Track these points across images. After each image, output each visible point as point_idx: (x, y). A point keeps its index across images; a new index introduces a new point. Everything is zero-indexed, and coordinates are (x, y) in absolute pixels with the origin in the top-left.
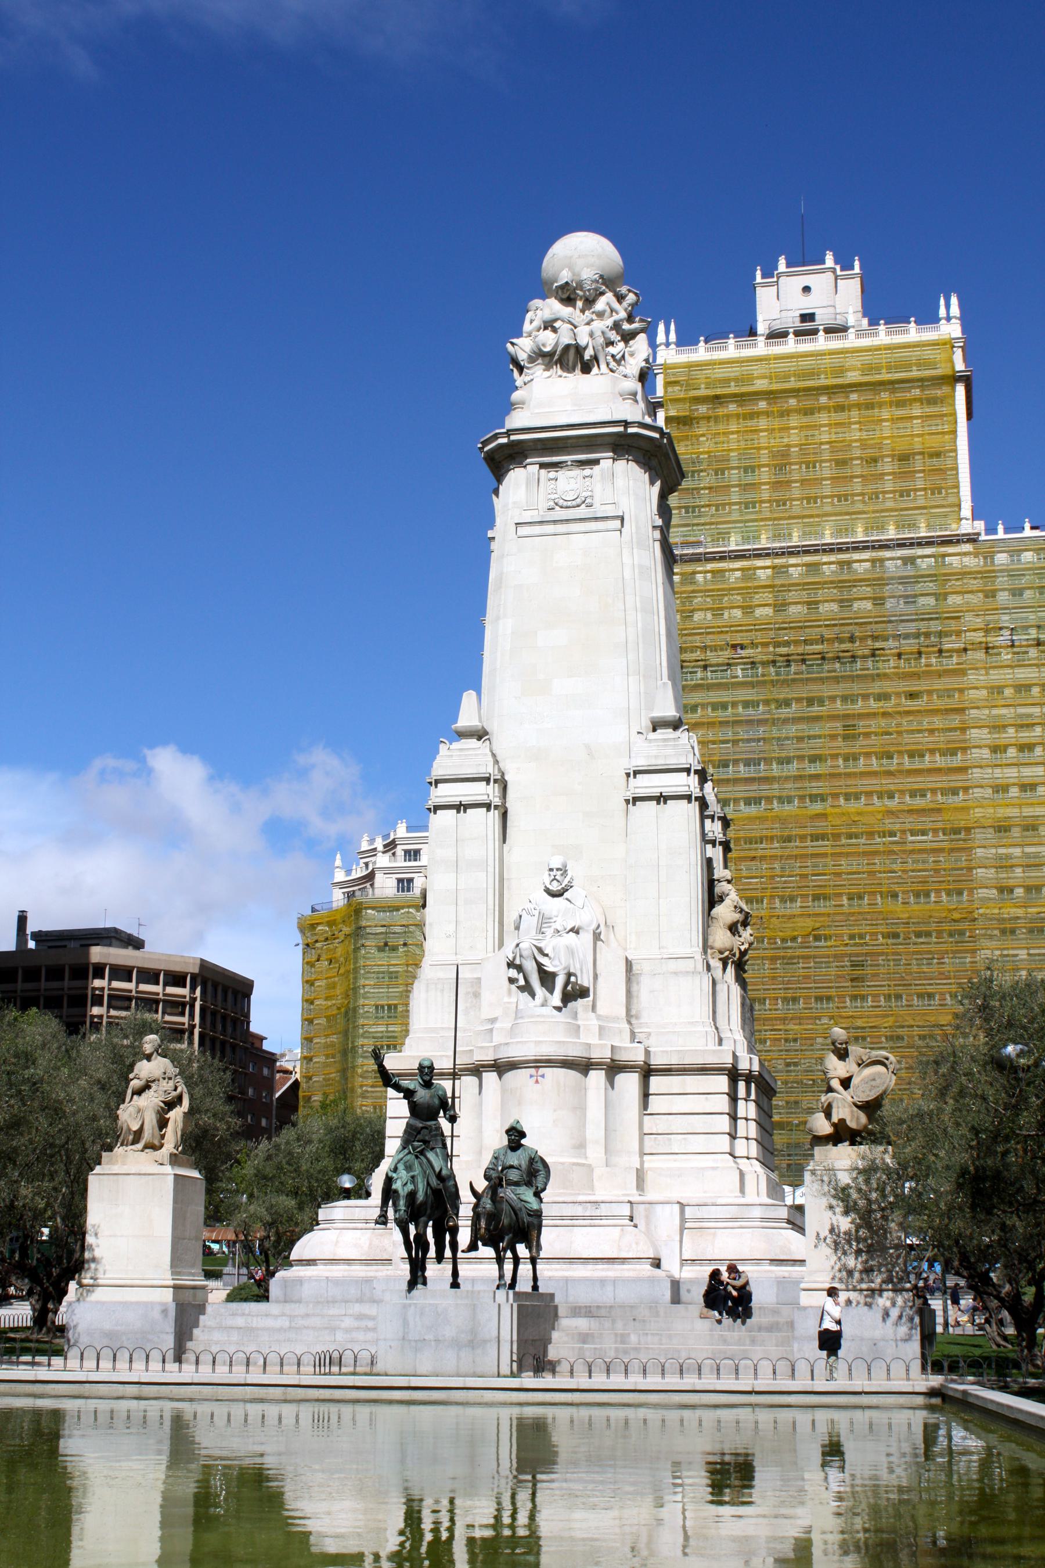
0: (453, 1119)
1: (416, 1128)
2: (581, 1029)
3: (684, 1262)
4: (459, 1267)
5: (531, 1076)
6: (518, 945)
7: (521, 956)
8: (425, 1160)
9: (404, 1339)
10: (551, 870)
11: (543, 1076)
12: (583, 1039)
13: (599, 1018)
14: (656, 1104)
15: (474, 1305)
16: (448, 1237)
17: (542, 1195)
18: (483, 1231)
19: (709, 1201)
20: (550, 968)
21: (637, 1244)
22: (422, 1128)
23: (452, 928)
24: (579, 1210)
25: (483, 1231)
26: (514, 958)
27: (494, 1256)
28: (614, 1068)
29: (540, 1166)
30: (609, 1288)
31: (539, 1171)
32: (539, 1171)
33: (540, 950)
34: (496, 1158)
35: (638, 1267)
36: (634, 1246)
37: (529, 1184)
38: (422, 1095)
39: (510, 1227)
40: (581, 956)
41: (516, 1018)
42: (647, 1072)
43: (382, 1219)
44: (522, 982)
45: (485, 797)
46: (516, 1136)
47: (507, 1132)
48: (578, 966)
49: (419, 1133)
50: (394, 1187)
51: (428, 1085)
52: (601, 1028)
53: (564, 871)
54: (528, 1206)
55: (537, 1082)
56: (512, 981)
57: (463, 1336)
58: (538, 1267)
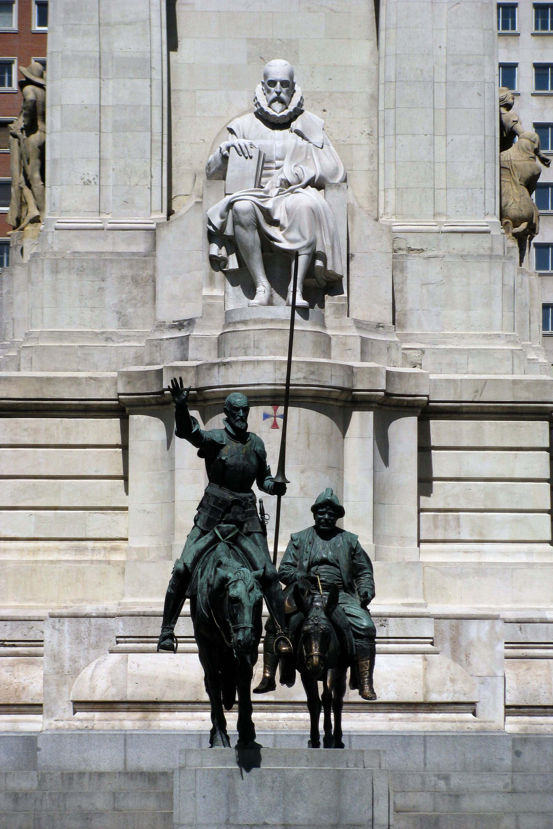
0: (279, 489)
1: (225, 501)
2: (333, 342)
3: (512, 710)
4: (255, 716)
5: (266, 416)
6: (230, 205)
7: (235, 223)
8: (239, 551)
9: (227, 822)
10: (273, 83)
12: (337, 358)
13: (359, 324)
14: (441, 463)
15: (340, 775)
17: (369, 607)
18: (316, 659)
19: (535, 615)
21: (453, 681)
23: (92, 170)
25: (316, 659)
26: (223, 225)
27: (304, 697)
28: (389, 407)
30: (417, 749)
31: (362, 568)
32: (363, 568)
33: (267, 213)
34: (296, 548)
35: (454, 716)
36: (449, 684)
37: (350, 589)
38: (230, 453)
39: (334, 656)
40: (332, 226)
41: (228, 324)
42: (427, 412)
43: (168, 642)
46: (328, 513)
47: (315, 509)
48: (327, 242)
49: (228, 510)
50: (233, 592)
51: (240, 434)
52: (364, 341)
53: (288, 85)
56: (216, 263)
57: (323, 817)
58: (344, 715)
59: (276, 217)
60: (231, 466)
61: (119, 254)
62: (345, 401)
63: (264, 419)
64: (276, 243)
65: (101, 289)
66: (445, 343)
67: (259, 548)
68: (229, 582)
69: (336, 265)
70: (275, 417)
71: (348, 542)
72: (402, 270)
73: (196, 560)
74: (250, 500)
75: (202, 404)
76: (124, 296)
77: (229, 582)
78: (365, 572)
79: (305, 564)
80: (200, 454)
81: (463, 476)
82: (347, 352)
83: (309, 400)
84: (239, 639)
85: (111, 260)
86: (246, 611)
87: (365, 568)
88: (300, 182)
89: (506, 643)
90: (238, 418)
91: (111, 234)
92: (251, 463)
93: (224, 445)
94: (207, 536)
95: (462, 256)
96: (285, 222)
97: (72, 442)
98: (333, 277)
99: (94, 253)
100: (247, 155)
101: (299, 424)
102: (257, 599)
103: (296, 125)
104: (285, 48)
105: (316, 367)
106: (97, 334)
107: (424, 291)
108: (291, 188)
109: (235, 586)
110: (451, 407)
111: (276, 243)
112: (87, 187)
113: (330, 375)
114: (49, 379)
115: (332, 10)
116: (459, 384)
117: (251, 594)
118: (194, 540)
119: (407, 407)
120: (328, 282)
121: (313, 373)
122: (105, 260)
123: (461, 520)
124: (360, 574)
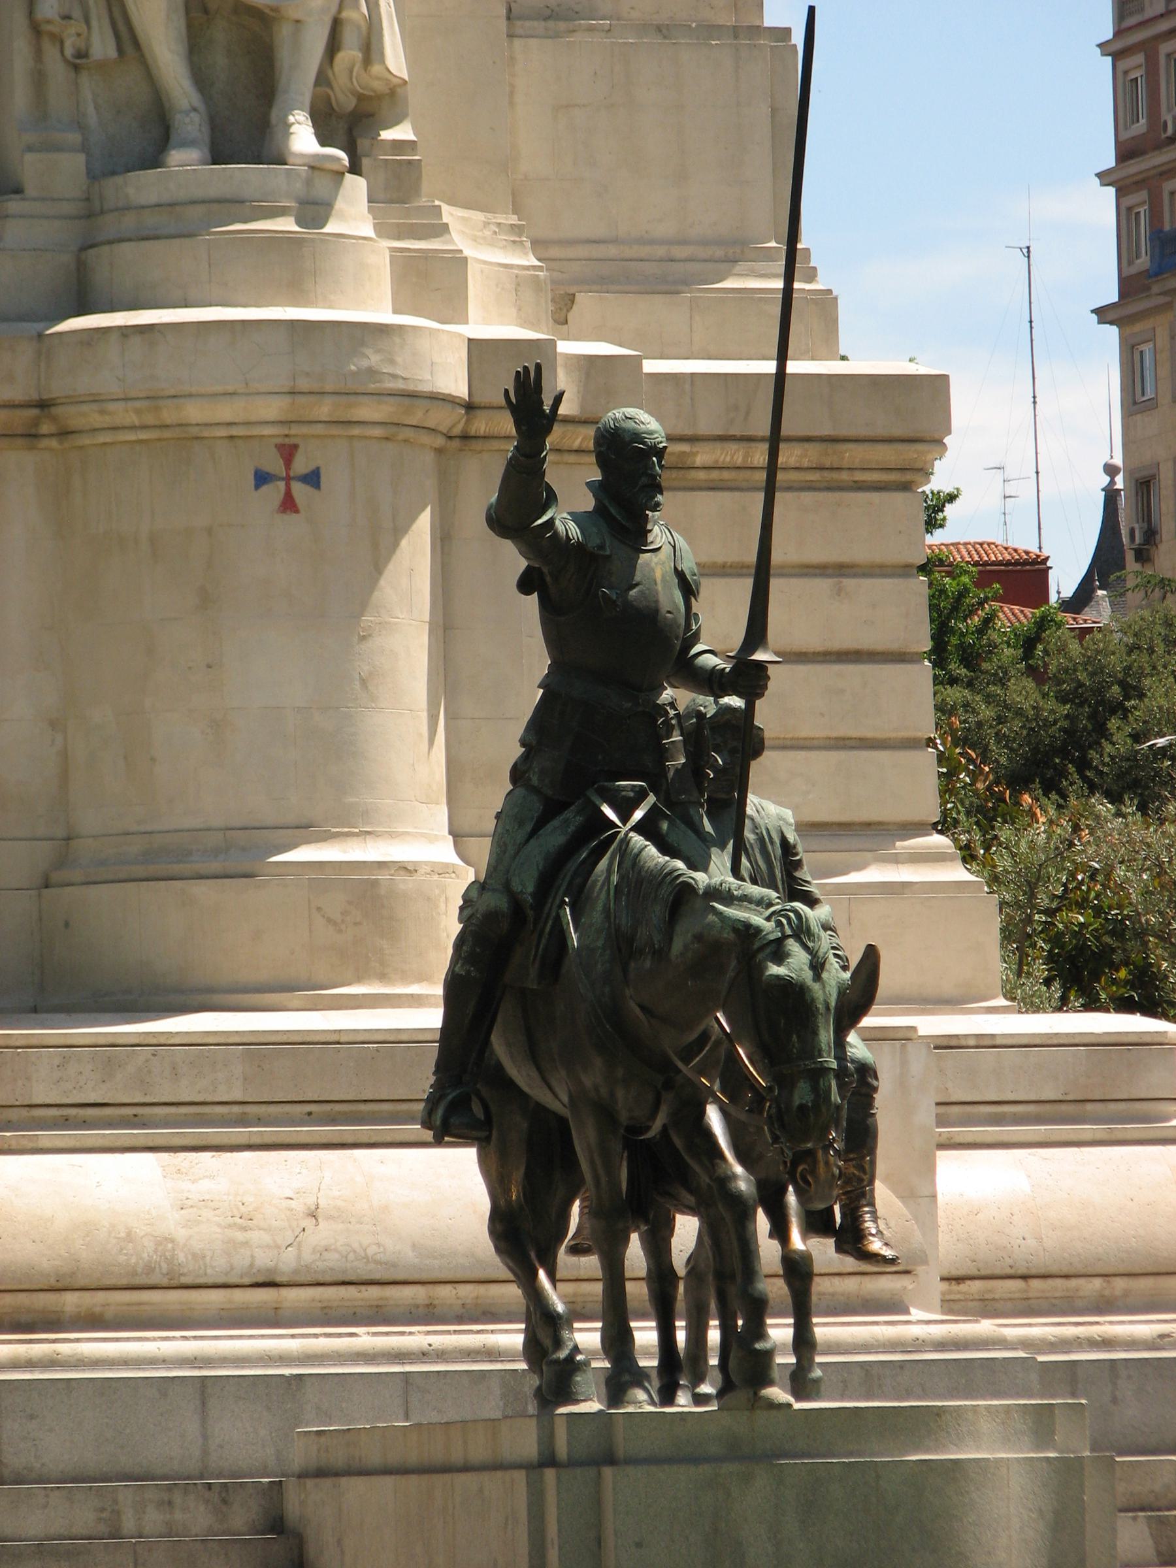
11: (313, 479)
44: (102, 46)
50: (775, 970)
55: (289, 504)
63: (257, 487)
68: (757, 945)
70: (288, 479)
73: (547, 883)
75: (54, 443)
77: (757, 945)
80: (526, 584)
83: (377, 432)
84: (797, 1101)
86: (821, 1021)
89: (937, 1104)
90: (644, 480)
93: (609, 557)
94: (568, 814)
95: (659, 29)
109: (780, 956)
118: (529, 827)
120: (361, 98)
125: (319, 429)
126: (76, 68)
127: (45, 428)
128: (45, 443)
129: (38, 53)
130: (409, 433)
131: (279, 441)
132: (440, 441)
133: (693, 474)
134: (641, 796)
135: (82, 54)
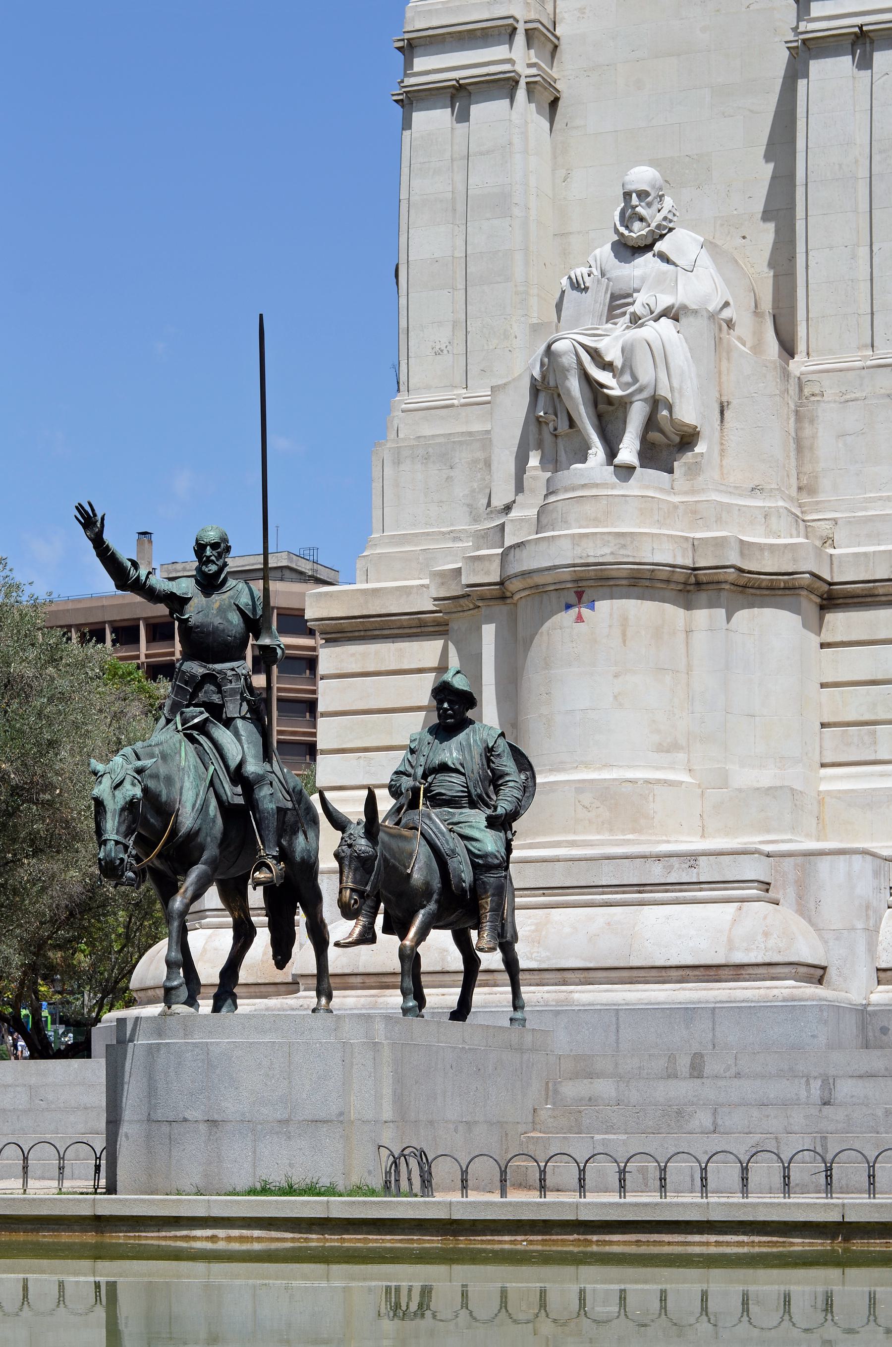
1: (193, 676)
16: (301, 918)
20: (614, 387)
22: (204, 676)
24: (656, 873)
29: (507, 764)
33: (595, 355)
44: (563, 426)
45: (507, 67)
54: (473, 846)
59: (608, 358)
60: (198, 627)
61: (470, 434)
62: (685, 584)
64: (605, 391)
65: (449, 479)
66: (865, 509)
67: (239, 740)
69: (687, 412)
71: (481, 740)
72: (812, 421)
74: (230, 673)
76: (475, 485)
78: (507, 779)
79: (420, 771)
81: (880, 677)
82: (698, 522)
83: (624, 582)
85: (459, 441)
86: (109, 815)
87: (507, 774)
88: (652, 313)
91: (464, 411)
92: (228, 621)
93: (190, 598)
96: (618, 363)
97: (406, 666)
98: (685, 429)
99: (442, 435)
100: (583, 286)
101: (611, 615)
102: (128, 799)
103: (659, 246)
104: (695, 166)
105: (629, 539)
106: (443, 533)
107: (840, 445)
108: (640, 322)
109: (100, 782)
110: (863, 589)
111: (605, 391)
112: (438, 357)
113: (651, 548)
114: (375, 591)
115: (751, 111)
116: (871, 558)
117: (117, 792)
119: (784, 589)
121: (624, 546)
122: (454, 442)
123: (878, 733)
124: (500, 782)
125: (591, 583)
126: (556, 436)
127: (508, 594)
128: (509, 601)
129: (540, 432)
130: (647, 583)
131: (575, 589)
132: (680, 587)
133: (878, 599)
134: (202, 713)
135: (555, 429)
